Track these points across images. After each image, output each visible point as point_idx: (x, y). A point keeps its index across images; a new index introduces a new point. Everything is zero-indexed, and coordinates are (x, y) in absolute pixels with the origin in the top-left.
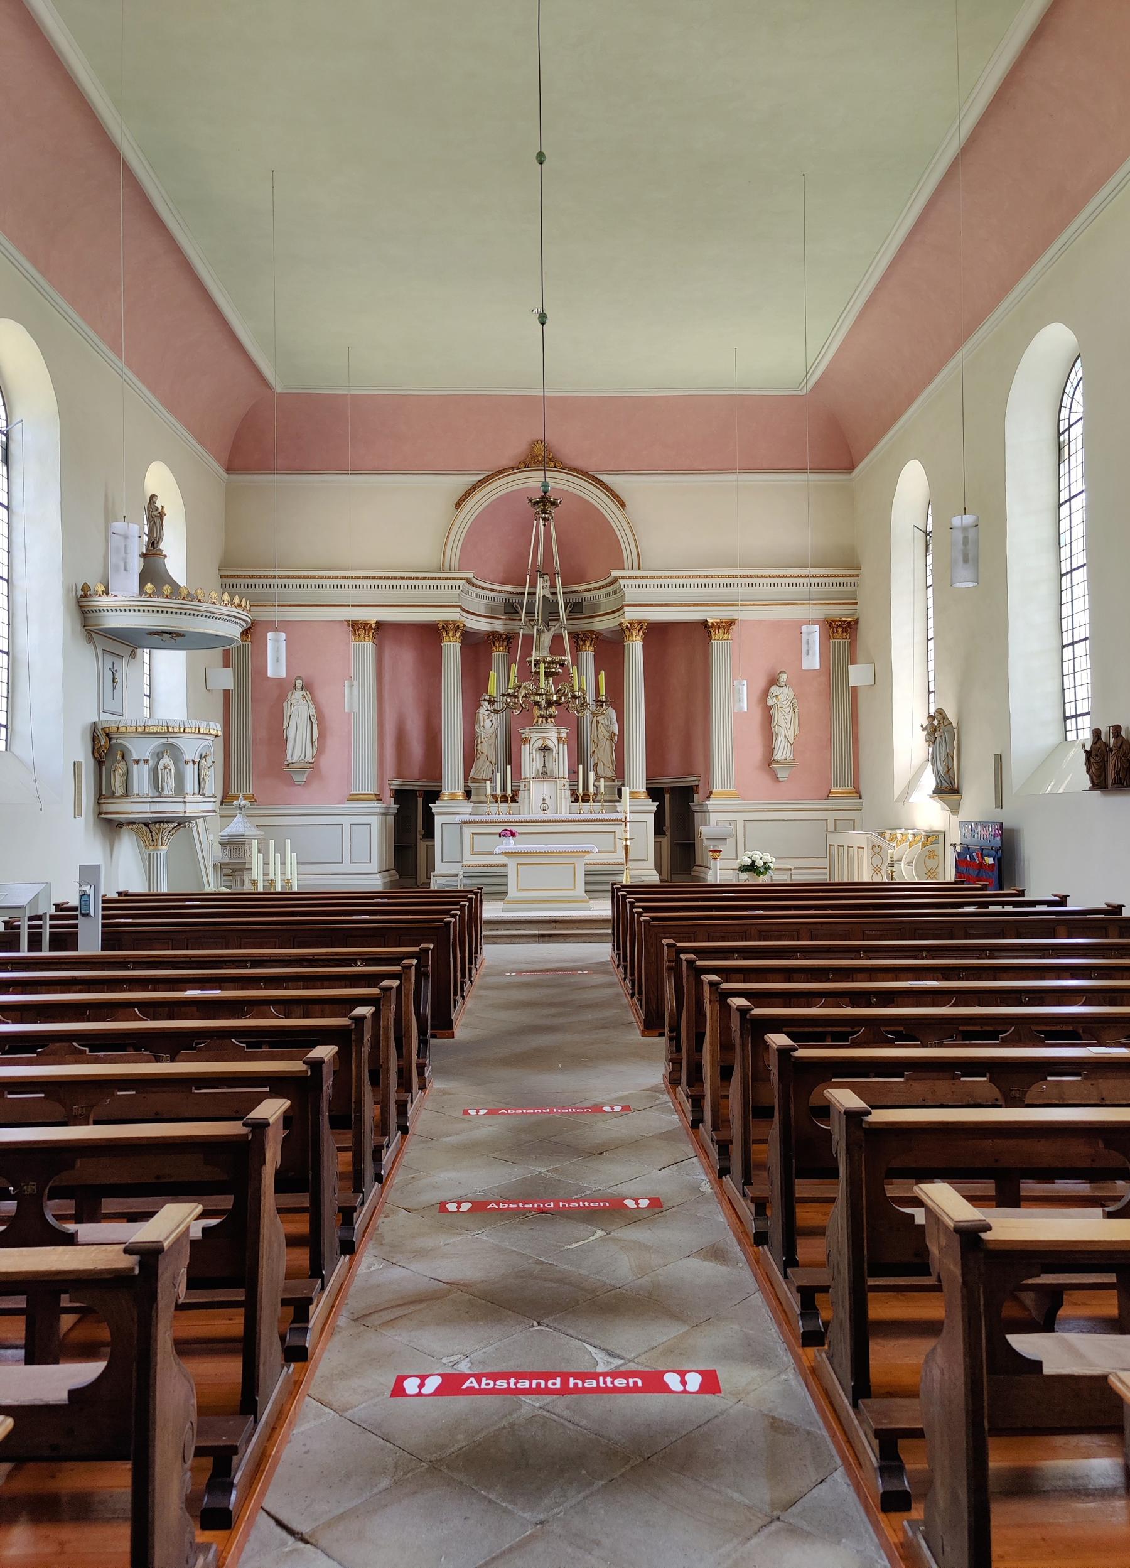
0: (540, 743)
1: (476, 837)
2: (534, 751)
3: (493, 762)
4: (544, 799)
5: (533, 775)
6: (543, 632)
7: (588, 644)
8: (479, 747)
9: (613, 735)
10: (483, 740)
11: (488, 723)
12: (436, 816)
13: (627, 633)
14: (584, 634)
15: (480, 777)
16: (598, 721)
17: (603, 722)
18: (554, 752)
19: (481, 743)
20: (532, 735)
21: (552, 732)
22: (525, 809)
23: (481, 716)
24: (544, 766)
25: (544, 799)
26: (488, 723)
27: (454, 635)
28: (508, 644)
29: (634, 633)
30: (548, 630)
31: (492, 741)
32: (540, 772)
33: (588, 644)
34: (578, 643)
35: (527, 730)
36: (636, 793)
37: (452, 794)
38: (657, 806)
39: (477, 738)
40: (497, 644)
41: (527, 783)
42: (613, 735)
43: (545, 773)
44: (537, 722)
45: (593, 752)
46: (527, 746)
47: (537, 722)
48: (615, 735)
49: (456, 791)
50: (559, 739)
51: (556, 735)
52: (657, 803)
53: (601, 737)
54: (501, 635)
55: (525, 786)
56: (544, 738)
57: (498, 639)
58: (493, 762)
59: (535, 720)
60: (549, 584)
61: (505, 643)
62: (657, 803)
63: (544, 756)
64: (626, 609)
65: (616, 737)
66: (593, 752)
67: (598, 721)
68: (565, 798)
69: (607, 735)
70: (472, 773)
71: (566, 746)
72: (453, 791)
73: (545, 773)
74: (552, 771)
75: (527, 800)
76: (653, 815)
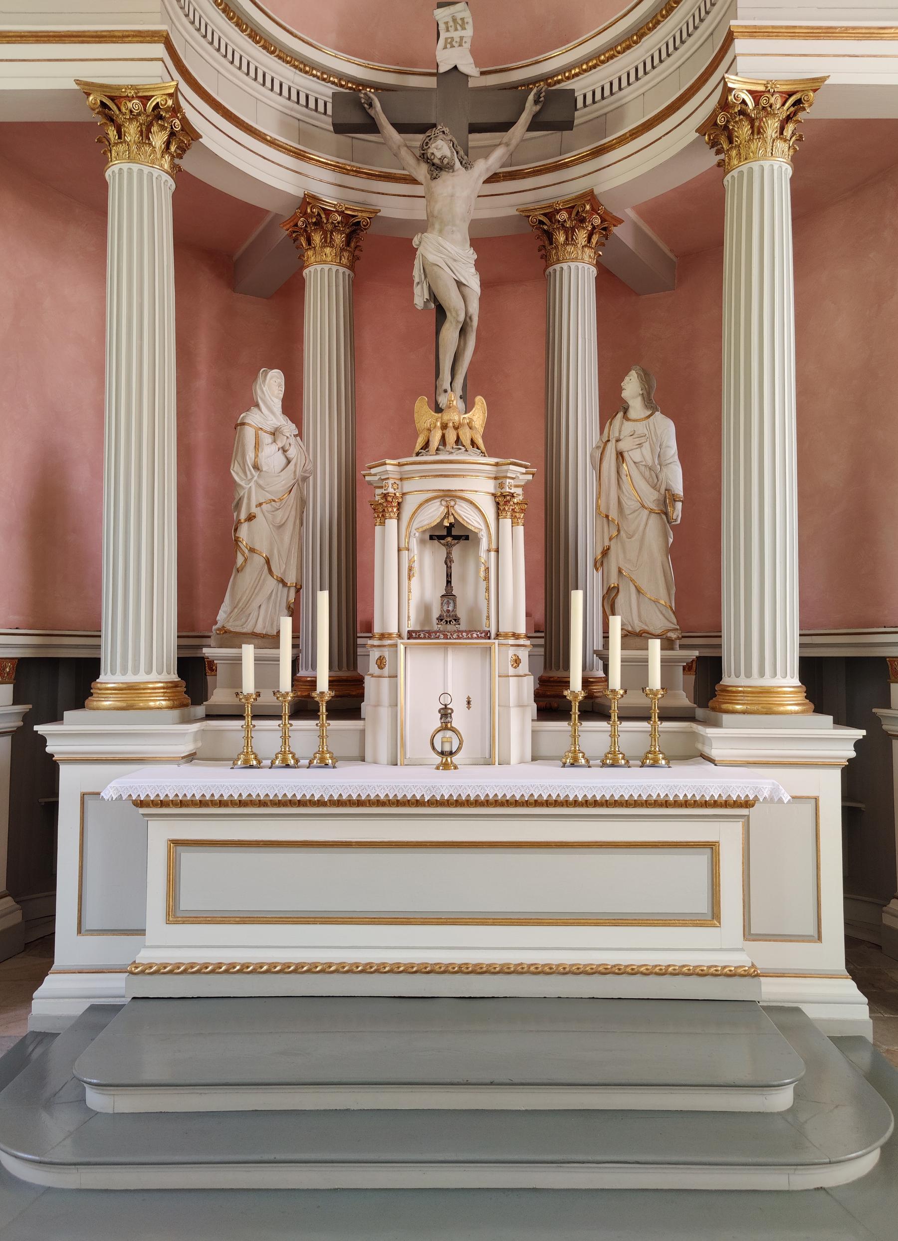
0: (433, 514)
1: (188, 857)
2: (414, 544)
3: (291, 579)
4: (445, 713)
5: (411, 624)
6: (450, 167)
7: (581, 236)
8: (244, 532)
9: (668, 498)
10: (254, 510)
11: (271, 456)
12: (65, 771)
13: (743, 131)
14: (570, 210)
15: (247, 629)
16: (620, 455)
17: (636, 455)
18: (484, 544)
19: (251, 518)
20: (407, 486)
21: (476, 474)
22: (379, 741)
23: (249, 434)
24: (449, 595)
25: (445, 713)
26: (271, 456)
27: (145, 134)
28: (348, 243)
29: (771, 126)
30: (467, 165)
31: (288, 512)
32: (436, 614)
33: (581, 236)
34: (549, 236)
35: (390, 467)
36: (766, 692)
37: (131, 688)
38: (858, 745)
39: (238, 506)
40: (317, 238)
41: (386, 653)
42: (668, 498)
43: (449, 618)
44: (426, 446)
45: (605, 552)
46: (392, 523)
47: (426, 446)
48: (674, 499)
49: (141, 677)
50: (501, 501)
51: (490, 486)
52: (860, 733)
53: (630, 504)
54: (328, 213)
55: (381, 663)
56: (448, 496)
57: (318, 224)
58: (291, 579)
59: (420, 442)
60: (469, 32)
61: (339, 239)
62: (860, 733)
63: (448, 561)
64: (740, 45)
65: (679, 505)
66: (605, 552)
67: (620, 455)
68: (521, 706)
69: (651, 497)
70: (221, 616)
71: (520, 529)
72: (130, 678)
73: (449, 618)
74: (474, 611)
75: (385, 713)
76: (836, 777)
